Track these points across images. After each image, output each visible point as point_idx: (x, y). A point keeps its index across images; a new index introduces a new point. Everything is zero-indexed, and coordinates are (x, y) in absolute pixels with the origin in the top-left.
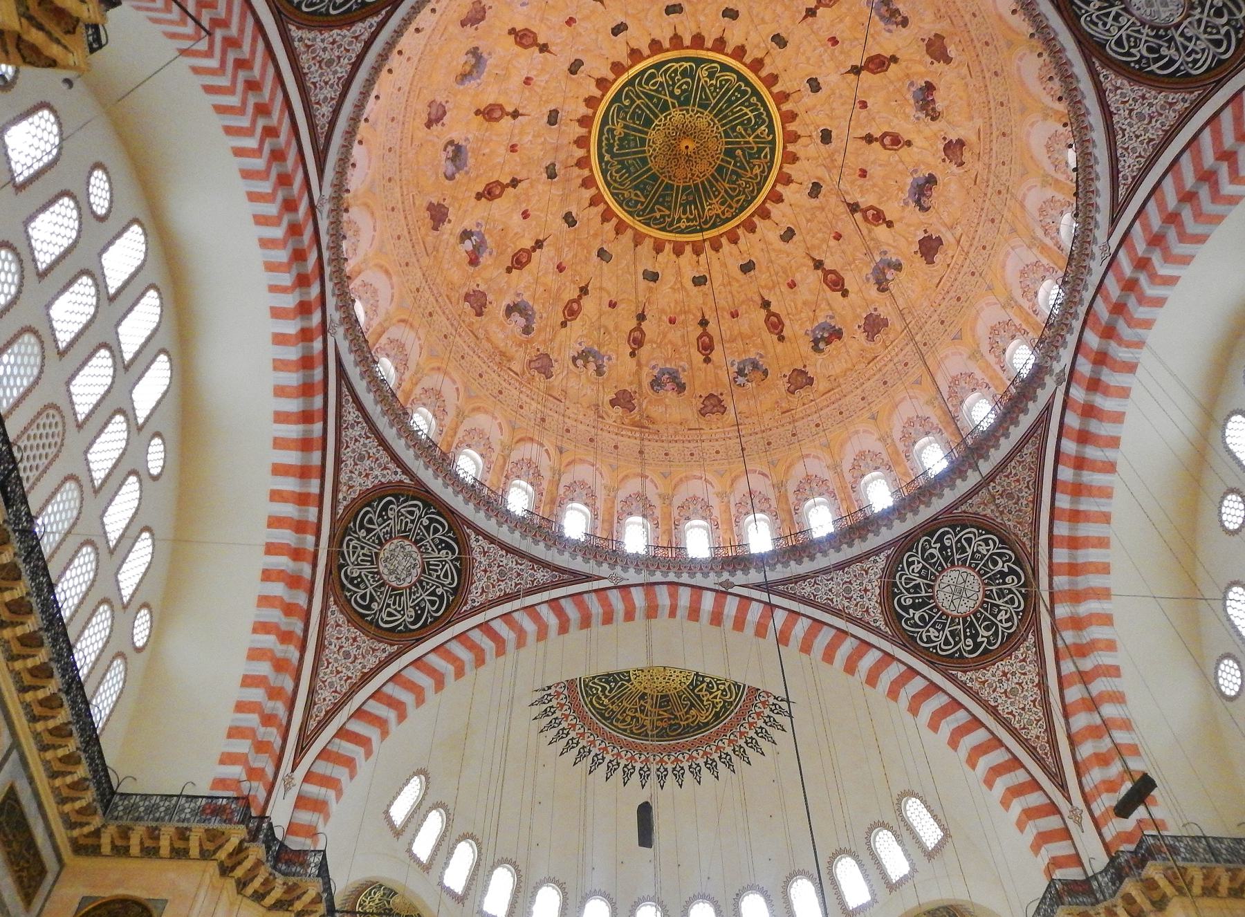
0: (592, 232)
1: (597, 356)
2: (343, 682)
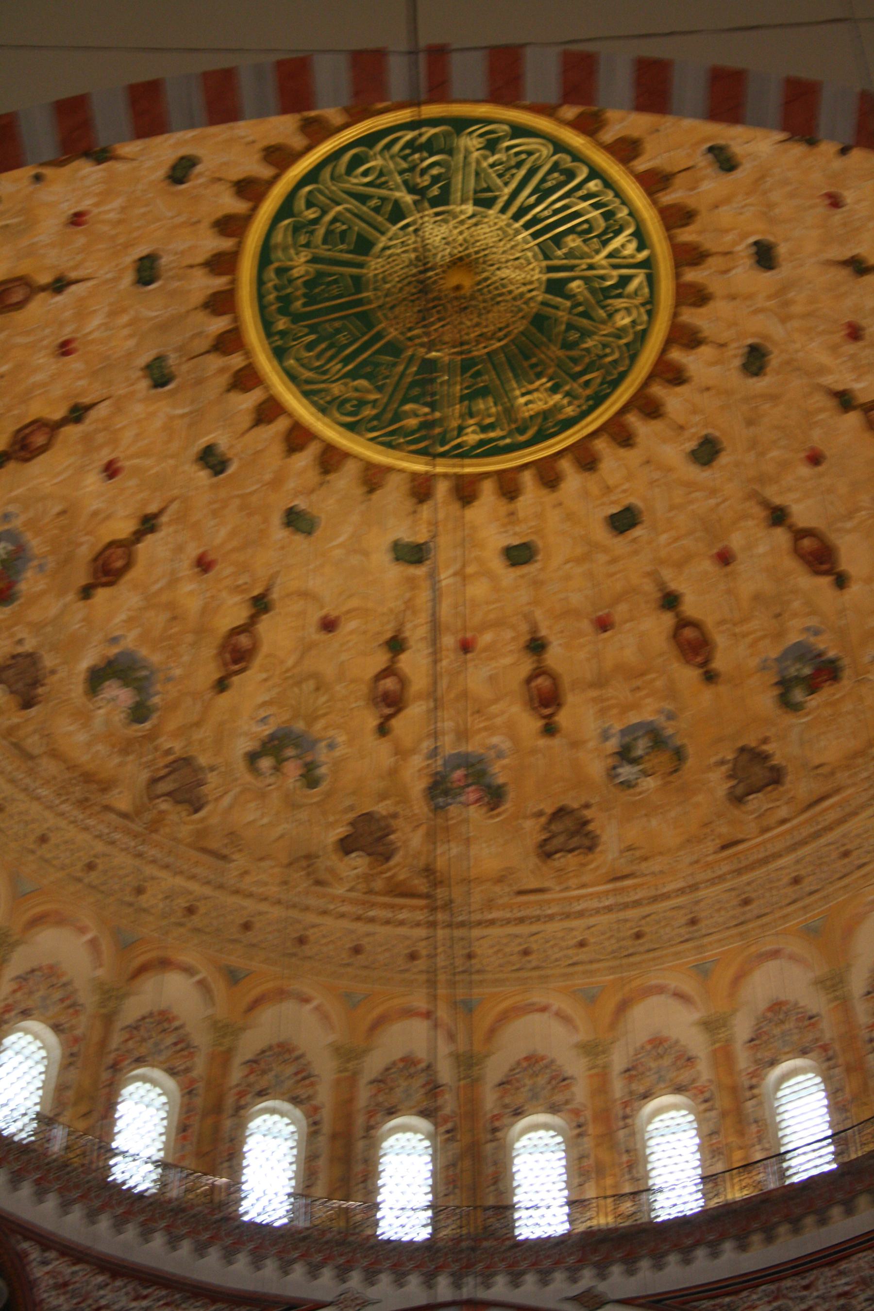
0: (268, 477)
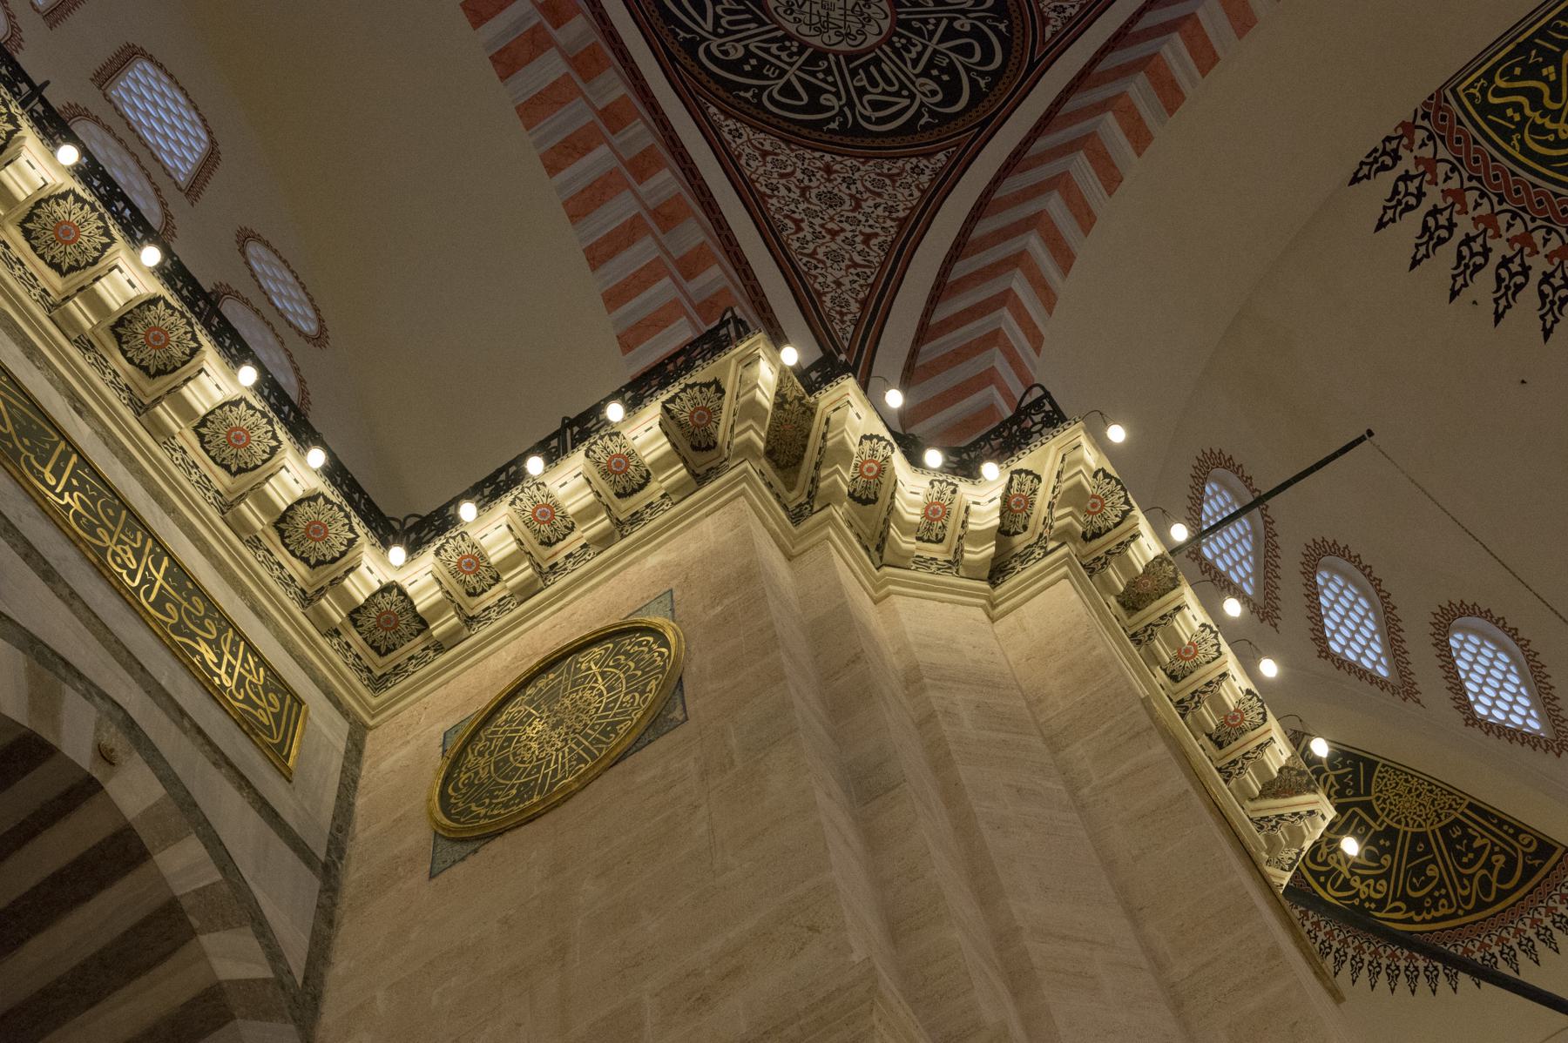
2: (860, 247)
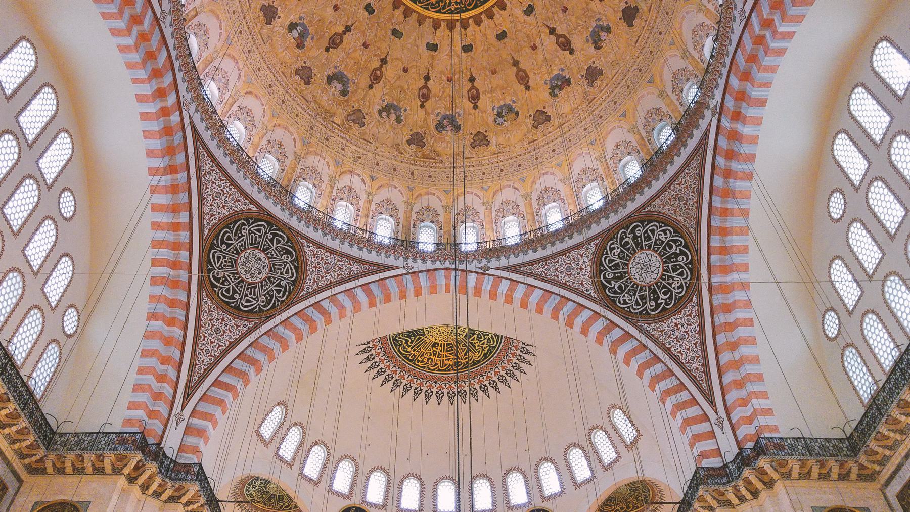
1: (396, 108)
2: (216, 349)
